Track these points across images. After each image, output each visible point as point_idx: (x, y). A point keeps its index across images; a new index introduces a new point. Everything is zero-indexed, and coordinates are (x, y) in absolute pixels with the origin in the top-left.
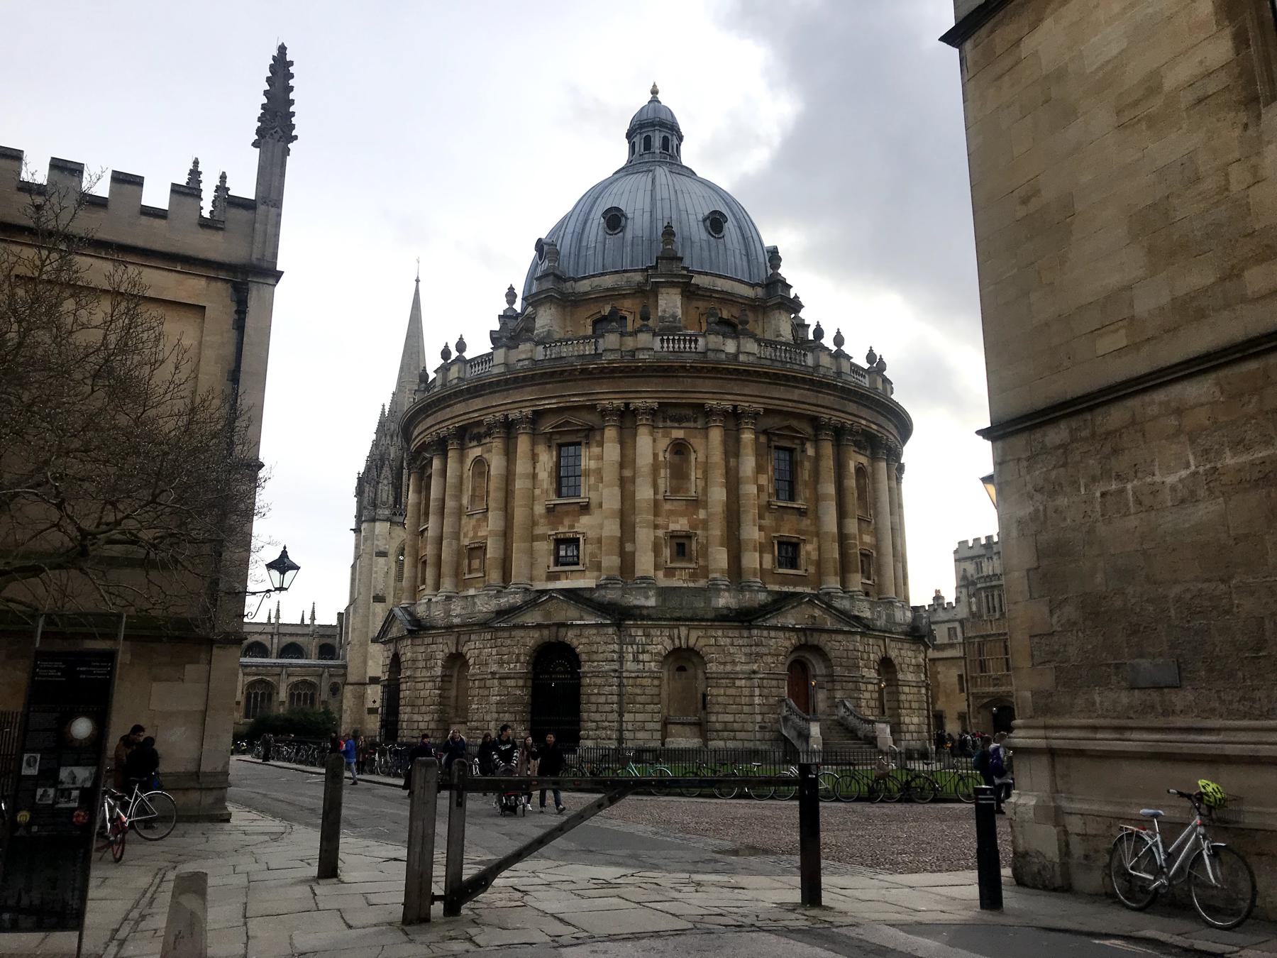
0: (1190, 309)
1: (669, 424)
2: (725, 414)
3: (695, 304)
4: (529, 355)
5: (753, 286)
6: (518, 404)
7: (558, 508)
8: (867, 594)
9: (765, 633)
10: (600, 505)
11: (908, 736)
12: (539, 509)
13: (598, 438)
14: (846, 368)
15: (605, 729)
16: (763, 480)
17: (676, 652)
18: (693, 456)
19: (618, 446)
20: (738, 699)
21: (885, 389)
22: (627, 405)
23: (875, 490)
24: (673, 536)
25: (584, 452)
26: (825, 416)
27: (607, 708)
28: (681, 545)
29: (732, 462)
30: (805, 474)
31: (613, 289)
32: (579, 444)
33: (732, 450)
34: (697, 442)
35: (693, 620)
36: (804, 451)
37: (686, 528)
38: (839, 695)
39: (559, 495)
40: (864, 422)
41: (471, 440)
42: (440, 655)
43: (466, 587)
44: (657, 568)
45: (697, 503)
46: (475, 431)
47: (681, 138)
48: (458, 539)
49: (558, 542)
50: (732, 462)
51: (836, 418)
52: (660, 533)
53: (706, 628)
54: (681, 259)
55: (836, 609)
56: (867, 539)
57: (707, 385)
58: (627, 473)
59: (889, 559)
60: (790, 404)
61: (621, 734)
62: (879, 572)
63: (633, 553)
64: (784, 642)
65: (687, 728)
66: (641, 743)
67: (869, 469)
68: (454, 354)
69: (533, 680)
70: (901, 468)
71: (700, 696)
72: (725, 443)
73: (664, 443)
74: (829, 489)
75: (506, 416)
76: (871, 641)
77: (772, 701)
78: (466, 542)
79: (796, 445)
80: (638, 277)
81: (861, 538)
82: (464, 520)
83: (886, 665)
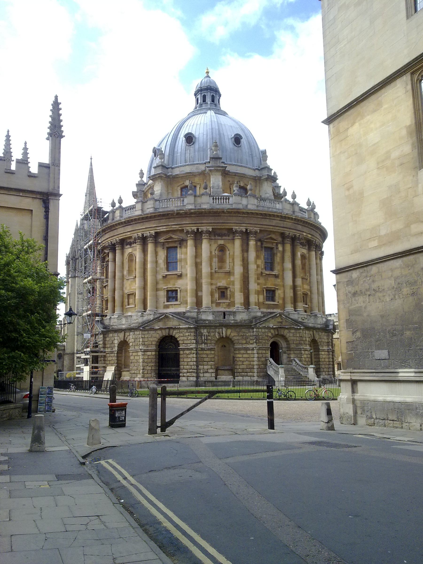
0: (395, 236)
1: (217, 237)
2: (241, 232)
3: (228, 179)
4: (152, 206)
5: (255, 170)
6: (149, 229)
7: (168, 277)
8: (306, 312)
9: (260, 330)
10: (187, 275)
11: (324, 374)
12: (160, 277)
13: (185, 244)
14: (297, 209)
15: (191, 372)
16: (259, 262)
17: (221, 338)
18: (228, 253)
19: (194, 248)
20: (248, 359)
21: (315, 218)
22: (198, 229)
23: (310, 265)
24: (219, 288)
25: (179, 250)
27: (192, 363)
28: (223, 292)
29: (245, 254)
30: (278, 259)
31: (190, 173)
32: (177, 247)
33: (245, 249)
34: (229, 246)
35: (228, 326)
36: (277, 248)
37: (225, 285)
38: (292, 356)
39: (168, 270)
40: (305, 234)
41: (127, 245)
42: (116, 342)
43: (127, 311)
44: (212, 302)
45: (229, 273)
46: (129, 241)
47: (220, 96)
48: (123, 290)
49: (168, 291)
50: (245, 254)
51: (292, 233)
52: (214, 287)
54: (220, 158)
55: (292, 319)
56: (306, 287)
57: (234, 220)
58: (198, 260)
59: (315, 297)
60: (271, 227)
62: (311, 302)
63: (202, 296)
65: (226, 372)
66: (206, 378)
67: (307, 255)
68: (117, 205)
69: (159, 352)
70: (322, 253)
71: (231, 358)
72: (242, 246)
73: (215, 246)
74: (288, 265)
75: (143, 235)
77: (263, 359)
78: (126, 291)
79: (274, 246)
80: (202, 168)
81: (303, 287)
82: (125, 280)
83: (314, 343)
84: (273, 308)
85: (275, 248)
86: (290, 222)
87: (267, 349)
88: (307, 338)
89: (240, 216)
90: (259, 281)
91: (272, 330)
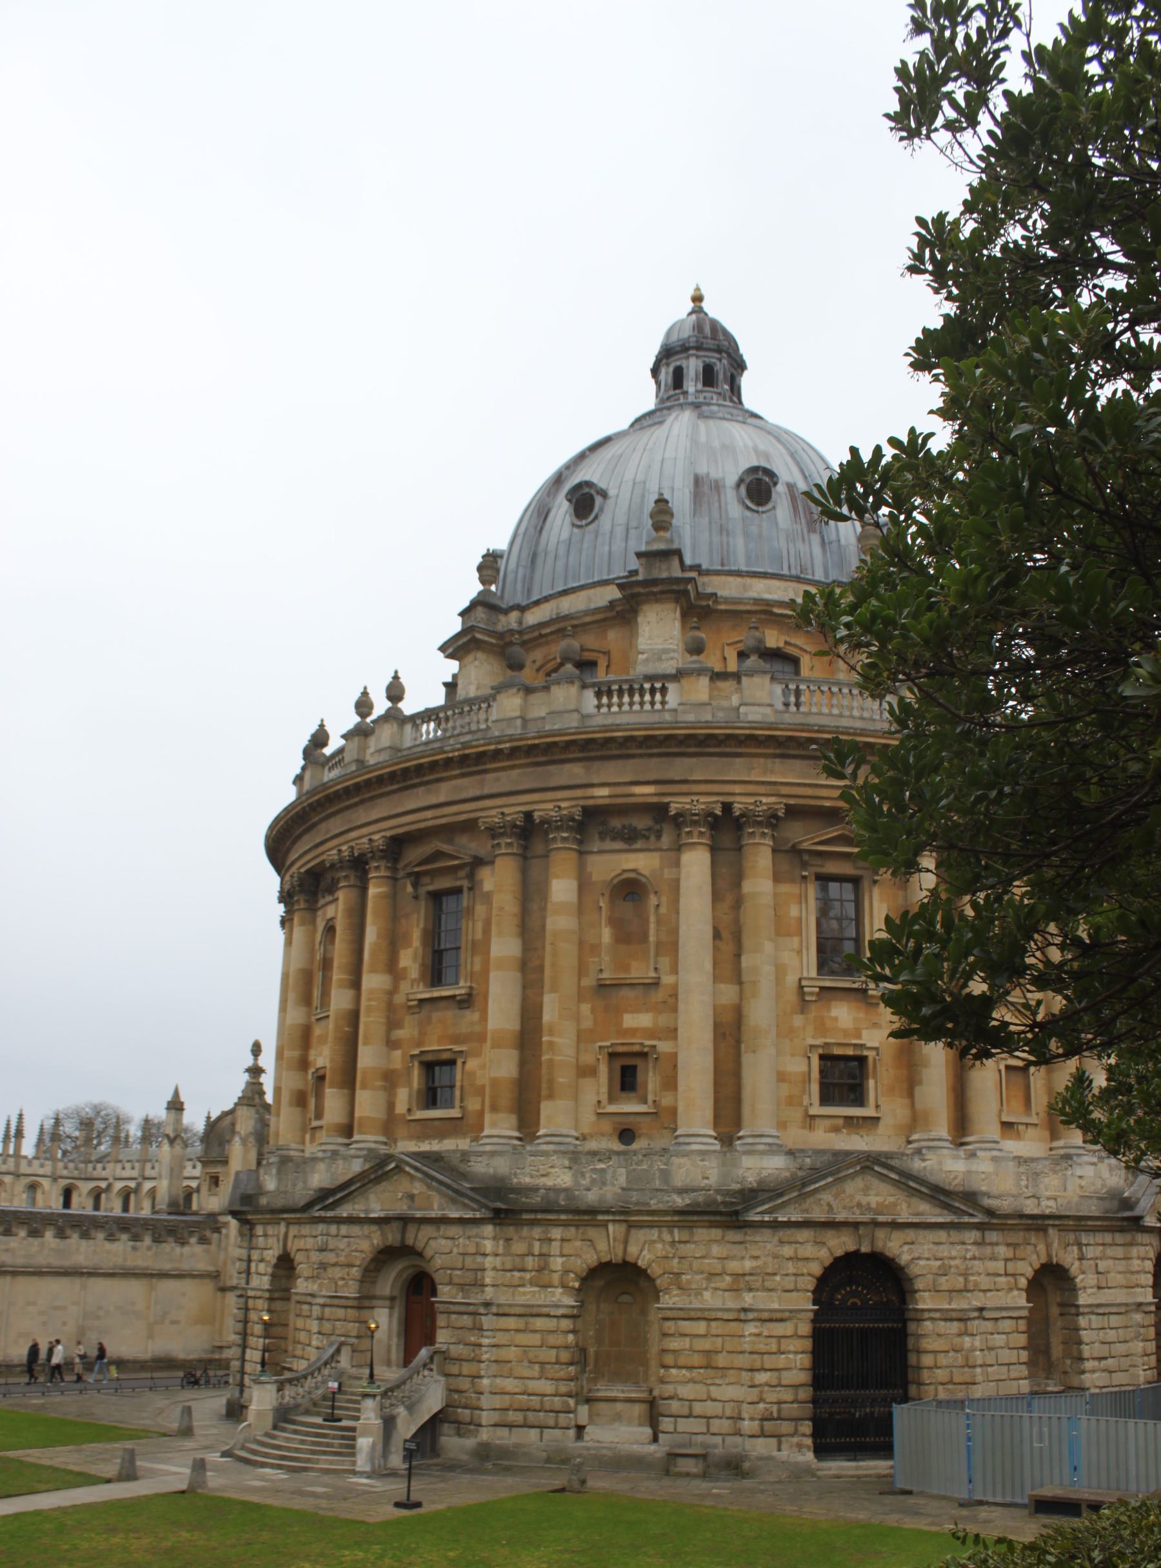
9: (333, 1229)
11: (684, 1425)
44: (304, 1130)
51: (513, 810)
53: (299, 1222)
60: (429, 814)
61: (242, 1379)
64: (364, 1243)
74: (505, 946)
76: (556, 1233)
84: (442, 1136)
85: (465, 884)
86: (512, 767)
87: (350, 1303)
88: (557, 1263)
89: (348, 808)
91: (374, 1228)
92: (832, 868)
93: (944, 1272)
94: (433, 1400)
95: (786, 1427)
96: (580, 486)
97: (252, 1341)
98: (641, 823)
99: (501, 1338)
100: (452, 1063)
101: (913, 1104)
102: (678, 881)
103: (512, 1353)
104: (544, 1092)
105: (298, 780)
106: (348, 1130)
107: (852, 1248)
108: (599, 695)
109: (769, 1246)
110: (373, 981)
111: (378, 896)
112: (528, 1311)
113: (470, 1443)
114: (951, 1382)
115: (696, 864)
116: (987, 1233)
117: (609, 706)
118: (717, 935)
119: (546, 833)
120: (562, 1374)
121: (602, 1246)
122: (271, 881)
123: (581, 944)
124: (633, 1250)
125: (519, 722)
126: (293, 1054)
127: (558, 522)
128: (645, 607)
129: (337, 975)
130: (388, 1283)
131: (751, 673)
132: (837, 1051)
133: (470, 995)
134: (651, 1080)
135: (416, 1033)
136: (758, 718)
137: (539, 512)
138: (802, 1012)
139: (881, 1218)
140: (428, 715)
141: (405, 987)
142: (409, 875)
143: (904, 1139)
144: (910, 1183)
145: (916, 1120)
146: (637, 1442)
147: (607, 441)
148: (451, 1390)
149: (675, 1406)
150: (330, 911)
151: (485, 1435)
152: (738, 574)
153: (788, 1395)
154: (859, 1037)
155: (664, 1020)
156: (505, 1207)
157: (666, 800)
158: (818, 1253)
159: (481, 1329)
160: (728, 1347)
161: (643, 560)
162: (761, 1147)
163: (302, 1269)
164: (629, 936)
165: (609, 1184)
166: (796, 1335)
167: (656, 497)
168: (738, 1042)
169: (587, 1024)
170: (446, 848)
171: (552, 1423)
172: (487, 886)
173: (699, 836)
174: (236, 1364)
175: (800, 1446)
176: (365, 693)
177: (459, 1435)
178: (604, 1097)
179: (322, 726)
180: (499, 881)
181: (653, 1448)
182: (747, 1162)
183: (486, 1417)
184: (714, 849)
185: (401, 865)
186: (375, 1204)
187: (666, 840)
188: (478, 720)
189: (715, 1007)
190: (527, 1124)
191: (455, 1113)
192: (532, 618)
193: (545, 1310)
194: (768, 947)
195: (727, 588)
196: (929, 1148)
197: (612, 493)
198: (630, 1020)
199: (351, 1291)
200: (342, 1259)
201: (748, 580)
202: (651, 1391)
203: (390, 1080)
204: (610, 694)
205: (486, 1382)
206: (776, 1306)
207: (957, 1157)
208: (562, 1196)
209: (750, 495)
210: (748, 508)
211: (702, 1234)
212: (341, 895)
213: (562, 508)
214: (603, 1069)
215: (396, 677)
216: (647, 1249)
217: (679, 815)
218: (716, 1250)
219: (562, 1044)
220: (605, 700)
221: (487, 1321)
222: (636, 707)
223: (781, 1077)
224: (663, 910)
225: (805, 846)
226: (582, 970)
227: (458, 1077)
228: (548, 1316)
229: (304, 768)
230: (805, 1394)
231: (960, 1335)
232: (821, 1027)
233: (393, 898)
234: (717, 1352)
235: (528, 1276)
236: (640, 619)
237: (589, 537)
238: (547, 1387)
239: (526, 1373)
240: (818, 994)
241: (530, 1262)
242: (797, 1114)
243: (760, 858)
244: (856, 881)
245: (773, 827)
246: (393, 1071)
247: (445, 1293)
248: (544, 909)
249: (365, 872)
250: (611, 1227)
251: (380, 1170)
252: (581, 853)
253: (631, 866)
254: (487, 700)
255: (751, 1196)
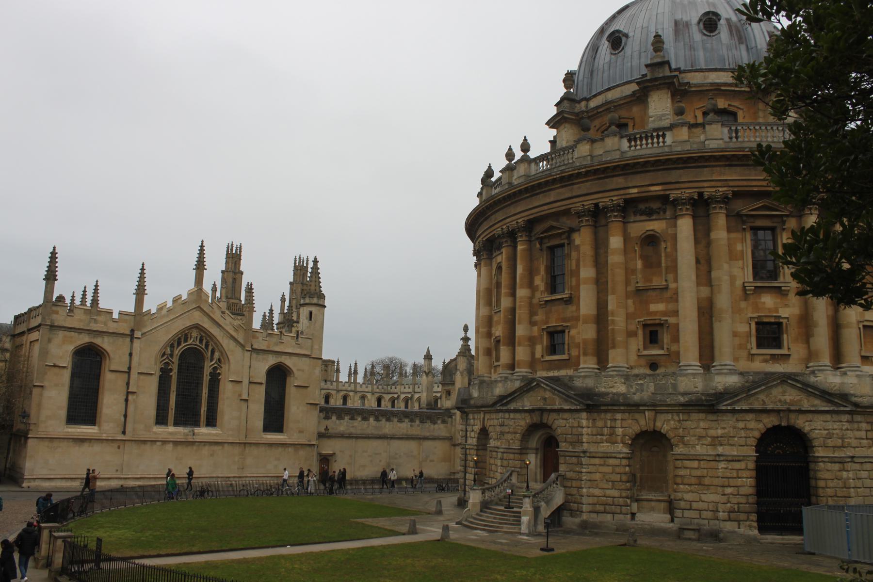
9: (507, 415)
11: (687, 514)
26: (577, 205)
51: (588, 203)
53: (490, 412)
60: (546, 207)
64: (522, 422)
74: (587, 272)
76: (619, 416)
84: (559, 368)
86: (587, 181)
88: (620, 431)
89: (504, 207)
90: (537, 318)
91: (527, 414)
92: (759, 223)
93: (830, 436)
94: (559, 499)
95: (743, 516)
96: (613, 33)
97: (469, 470)
98: (655, 205)
99: (592, 469)
100: (563, 332)
101: (809, 347)
102: (676, 234)
103: (597, 476)
104: (610, 345)
105: (480, 195)
106: (512, 367)
107: (776, 423)
108: (629, 141)
109: (731, 422)
110: (522, 293)
111: (523, 250)
112: (605, 455)
113: (577, 520)
114: (836, 496)
115: (685, 226)
116: (854, 416)
117: (636, 146)
118: (698, 261)
119: (606, 213)
120: (623, 487)
121: (642, 422)
122: (469, 245)
123: (626, 269)
124: (659, 424)
125: (589, 158)
126: (483, 330)
127: (603, 52)
128: (652, 93)
129: (504, 290)
130: (534, 442)
131: (710, 123)
132: (766, 320)
133: (571, 297)
134: (666, 338)
135: (544, 318)
136: (716, 146)
137: (593, 48)
138: (745, 300)
139: (792, 408)
140: (542, 158)
141: (538, 295)
142: (538, 239)
143: (803, 366)
144: (808, 389)
145: (811, 355)
146: (662, 522)
147: (626, 7)
148: (567, 494)
149: (682, 504)
150: (499, 259)
151: (585, 517)
152: (701, 70)
153: (743, 500)
154: (778, 312)
155: (671, 306)
156: (592, 403)
157: (668, 193)
158: (757, 426)
159: (582, 464)
160: (710, 474)
161: (649, 68)
162: (725, 371)
163: (492, 435)
164: (652, 264)
165: (646, 390)
166: (746, 469)
167: (654, 34)
168: (711, 317)
169: (631, 309)
170: (554, 224)
171: (619, 511)
172: (577, 242)
173: (687, 210)
174: (461, 481)
175: (750, 527)
176: (510, 149)
177: (572, 516)
178: (641, 347)
179: (490, 167)
180: (583, 239)
181: (671, 525)
182: (718, 379)
183: (585, 508)
184: (694, 217)
185: (533, 234)
186: (527, 402)
187: (669, 214)
188: (568, 158)
189: (698, 299)
190: (602, 362)
191: (565, 357)
192: (593, 104)
193: (614, 455)
194: (726, 266)
195: (695, 79)
196: (819, 370)
197: (630, 35)
198: (653, 307)
199: (516, 445)
200: (512, 430)
201: (707, 74)
202: (669, 496)
203: (532, 341)
204: (635, 140)
205: (584, 490)
206: (735, 453)
207: (835, 375)
208: (621, 397)
209: (705, 27)
210: (705, 35)
211: (695, 416)
212: (504, 250)
213: (605, 45)
214: (640, 333)
215: (525, 140)
216: (666, 424)
217: (674, 200)
218: (702, 424)
219: (618, 321)
220: (633, 143)
221: (584, 460)
222: (650, 146)
223: (735, 334)
224: (668, 250)
225: (744, 212)
226: (627, 282)
227: (566, 339)
228: (615, 458)
229: (482, 189)
230: (752, 499)
231: (840, 471)
232: (756, 308)
233: (530, 251)
234: (704, 477)
235: (605, 438)
236: (649, 100)
237: (620, 59)
238: (616, 493)
239: (606, 486)
240: (754, 290)
241: (606, 431)
242: (744, 354)
243: (720, 220)
244: (773, 229)
245: (726, 203)
246: (534, 337)
247: (563, 446)
248: (607, 252)
249: (516, 239)
250: (647, 413)
251: (529, 386)
252: (624, 223)
253: (651, 228)
254: (572, 148)
255: (721, 396)
